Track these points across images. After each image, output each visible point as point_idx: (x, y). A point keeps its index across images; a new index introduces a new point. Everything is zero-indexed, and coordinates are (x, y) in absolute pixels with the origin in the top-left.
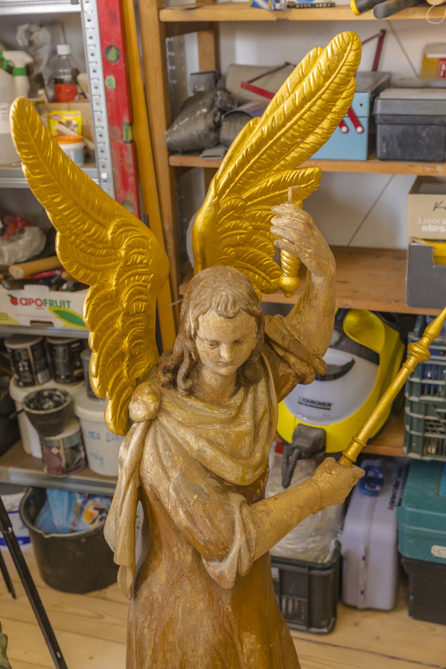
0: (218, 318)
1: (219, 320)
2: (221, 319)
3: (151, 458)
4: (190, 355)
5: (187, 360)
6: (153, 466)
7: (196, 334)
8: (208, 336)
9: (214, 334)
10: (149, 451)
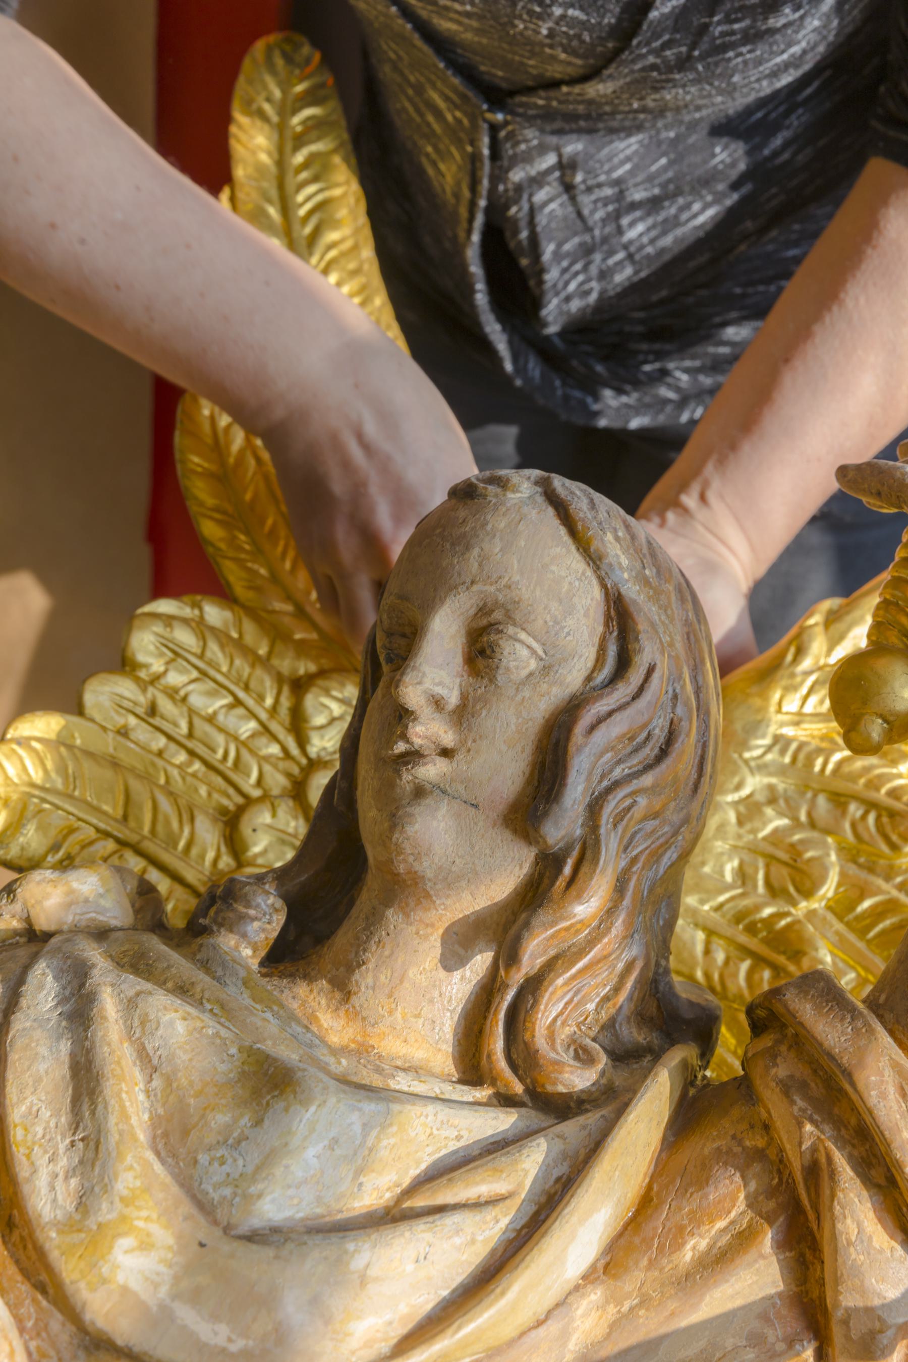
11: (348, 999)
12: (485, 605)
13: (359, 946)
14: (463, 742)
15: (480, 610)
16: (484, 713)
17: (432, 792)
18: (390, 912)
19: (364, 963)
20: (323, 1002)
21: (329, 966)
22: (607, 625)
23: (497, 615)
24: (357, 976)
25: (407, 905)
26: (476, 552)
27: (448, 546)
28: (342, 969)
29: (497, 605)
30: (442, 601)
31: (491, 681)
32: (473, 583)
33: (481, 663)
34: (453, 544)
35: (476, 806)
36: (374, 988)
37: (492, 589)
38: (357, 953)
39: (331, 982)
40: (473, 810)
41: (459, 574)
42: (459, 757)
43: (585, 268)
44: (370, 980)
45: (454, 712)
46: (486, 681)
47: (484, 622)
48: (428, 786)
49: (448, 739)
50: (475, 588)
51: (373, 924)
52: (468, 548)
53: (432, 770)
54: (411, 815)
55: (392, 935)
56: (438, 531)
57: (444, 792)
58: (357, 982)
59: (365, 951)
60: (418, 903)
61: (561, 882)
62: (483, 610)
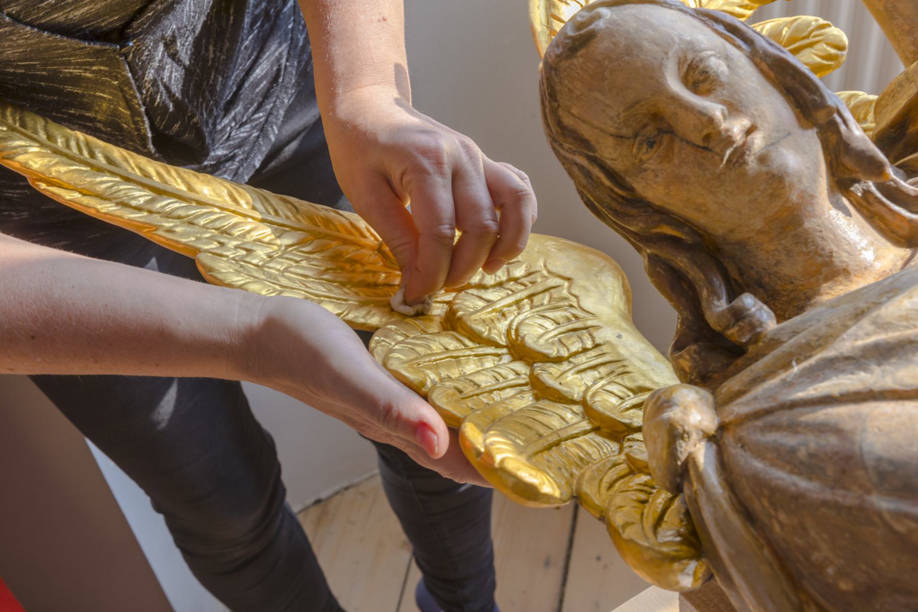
0: (575, 61)
1: (581, 60)
2: (582, 56)
3: (782, 516)
5: (682, 261)
6: (804, 529)
7: (611, 174)
8: (610, 123)
9: (608, 102)
10: (763, 506)
12: (679, 59)
13: (816, 253)
14: (753, 116)
15: (679, 63)
16: (743, 96)
17: (768, 151)
18: (807, 225)
19: (831, 253)
20: (841, 287)
21: (813, 280)
22: (708, 26)
23: (690, 56)
24: (836, 261)
25: (809, 212)
26: (646, 44)
27: (627, 58)
28: (824, 270)
30: (665, 78)
31: (720, 86)
32: (666, 53)
33: (704, 87)
34: (628, 55)
35: (789, 134)
36: (850, 254)
38: (821, 255)
39: (827, 279)
41: (655, 58)
42: (759, 123)
43: (204, 98)
44: (844, 255)
45: (730, 113)
46: (719, 89)
47: (686, 67)
48: (764, 151)
49: (746, 122)
50: (670, 54)
51: (806, 239)
52: (639, 47)
56: (606, 63)
57: (772, 144)
58: (841, 262)
59: (823, 249)
60: (812, 204)
61: (843, 128)
62: (680, 63)
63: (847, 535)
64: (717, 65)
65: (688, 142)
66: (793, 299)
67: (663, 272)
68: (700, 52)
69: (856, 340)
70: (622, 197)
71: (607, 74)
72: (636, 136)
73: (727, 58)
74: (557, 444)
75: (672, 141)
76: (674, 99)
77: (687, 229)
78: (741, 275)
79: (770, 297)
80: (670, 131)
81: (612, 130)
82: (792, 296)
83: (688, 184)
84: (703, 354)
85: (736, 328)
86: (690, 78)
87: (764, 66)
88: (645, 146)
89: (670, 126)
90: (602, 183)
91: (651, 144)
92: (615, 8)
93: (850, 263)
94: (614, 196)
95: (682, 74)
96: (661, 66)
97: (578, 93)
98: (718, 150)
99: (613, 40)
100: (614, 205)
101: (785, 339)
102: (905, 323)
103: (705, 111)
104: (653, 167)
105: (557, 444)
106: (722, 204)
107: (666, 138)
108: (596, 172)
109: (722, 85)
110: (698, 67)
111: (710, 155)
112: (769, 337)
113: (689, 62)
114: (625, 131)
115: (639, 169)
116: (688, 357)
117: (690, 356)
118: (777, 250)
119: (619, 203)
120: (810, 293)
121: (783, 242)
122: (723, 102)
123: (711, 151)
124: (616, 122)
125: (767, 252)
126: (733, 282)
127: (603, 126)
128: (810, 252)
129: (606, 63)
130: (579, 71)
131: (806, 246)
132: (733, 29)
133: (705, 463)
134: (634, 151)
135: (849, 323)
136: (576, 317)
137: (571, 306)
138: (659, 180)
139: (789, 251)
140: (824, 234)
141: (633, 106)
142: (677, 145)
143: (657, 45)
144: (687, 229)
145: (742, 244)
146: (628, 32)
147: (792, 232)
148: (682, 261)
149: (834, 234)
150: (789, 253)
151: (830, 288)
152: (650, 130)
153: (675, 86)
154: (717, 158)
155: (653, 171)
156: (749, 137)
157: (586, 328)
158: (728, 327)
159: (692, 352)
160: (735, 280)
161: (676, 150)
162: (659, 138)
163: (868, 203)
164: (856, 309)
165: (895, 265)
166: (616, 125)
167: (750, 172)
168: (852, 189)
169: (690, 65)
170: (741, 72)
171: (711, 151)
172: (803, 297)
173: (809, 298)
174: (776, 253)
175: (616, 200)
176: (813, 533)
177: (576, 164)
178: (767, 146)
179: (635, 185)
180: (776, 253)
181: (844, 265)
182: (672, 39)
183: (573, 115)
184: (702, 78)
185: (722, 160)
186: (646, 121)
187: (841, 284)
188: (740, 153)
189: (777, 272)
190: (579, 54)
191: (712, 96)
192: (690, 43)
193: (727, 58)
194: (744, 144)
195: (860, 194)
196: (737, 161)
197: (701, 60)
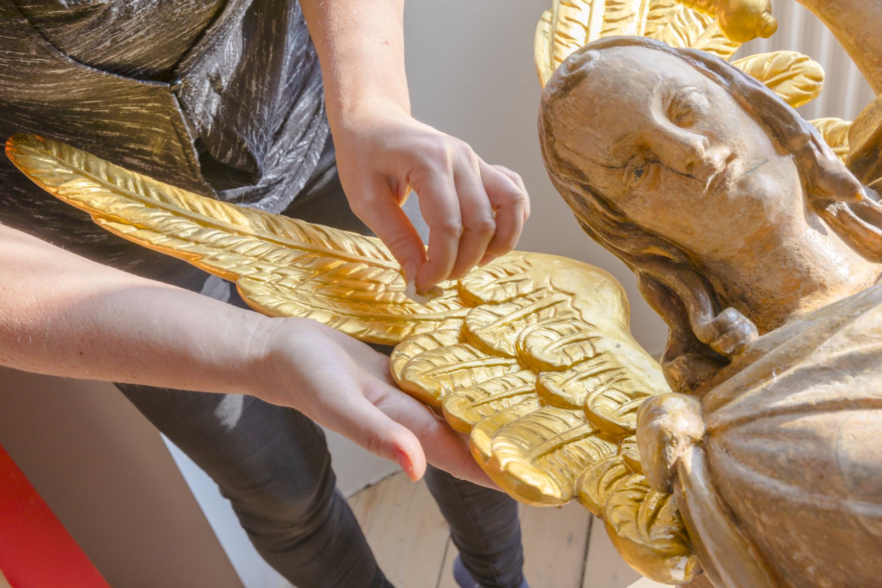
1: (573, 99)
2: (574, 94)
3: (764, 518)
4: (663, 261)
5: (670, 279)
6: (785, 530)
8: (600, 154)
9: (598, 136)
10: (747, 509)
11: (825, 286)
12: (663, 95)
13: (795, 269)
15: (663, 99)
16: (723, 127)
18: (785, 244)
19: (809, 269)
21: (792, 294)
22: (690, 63)
24: (814, 277)
26: (632, 82)
27: (615, 95)
28: (802, 285)
29: (668, 88)
31: (702, 118)
32: (651, 90)
33: (686, 119)
34: (616, 92)
35: (767, 161)
36: (826, 270)
37: (660, 84)
38: (799, 272)
39: (805, 294)
40: (768, 164)
41: (641, 95)
42: (738, 152)
45: (711, 142)
46: (700, 121)
47: (669, 102)
48: (743, 177)
49: (726, 151)
50: (655, 91)
51: (785, 257)
52: (626, 85)
53: (738, 169)
54: (760, 189)
55: (800, 248)
57: (751, 170)
58: (817, 277)
59: (801, 266)
60: (790, 225)
61: (817, 153)
62: (664, 99)
63: (825, 537)
64: (698, 99)
65: (673, 171)
66: (774, 312)
67: (653, 289)
68: (682, 88)
69: (832, 351)
70: (615, 222)
71: (597, 111)
72: (625, 166)
73: (708, 93)
74: (560, 447)
75: (658, 171)
76: (659, 132)
77: (674, 250)
78: (726, 290)
79: (753, 311)
80: (656, 161)
81: (603, 161)
82: (773, 309)
83: (674, 208)
84: (691, 364)
85: (721, 340)
86: (674, 112)
87: (742, 99)
88: (634, 175)
89: (657, 156)
90: (595, 209)
91: (639, 173)
92: (603, 51)
93: (826, 278)
94: (607, 221)
95: (666, 109)
96: (647, 102)
97: (572, 128)
98: (700, 177)
99: (603, 79)
100: (607, 228)
101: (766, 350)
102: (878, 336)
103: (687, 142)
104: (641, 194)
105: (560, 447)
106: (706, 226)
107: (653, 167)
108: (590, 199)
109: (703, 117)
110: (680, 102)
111: (693, 182)
112: (751, 348)
113: (672, 98)
114: (615, 162)
115: (629, 195)
116: (677, 367)
117: (680, 366)
118: (758, 267)
119: (612, 227)
120: (789, 306)
121: (763, 260)
122: (705, 133)
123: (694, 178)
124: (606, 154)
125: (749, 269)
126: (718, 297)
127: (595, 158)
128: (788, 269)
129: (596, 100)
130: (572, 108)
131: (785, 263)
132: (713, 66)
133: (693, 466)
134: (624, 179)
135: (826, 335)
136: (579, 329)
137: (574, 319)
138: (647, 205)
139: (769, 268)
140: (802, 252)
141: (621, 139)
142: (663, 173)
143: (642, 83)
144: (674, 250)
145: (725, 262)
146: (615, 72)
147: (772, 251)
148: (670, 279)
149: (811, 252)
150: (769, 270)
151: (808, 302)
152: (638, 161)
153: (660, 119)
154: (700, 184)
155: (642, 197)
156: (729, 165)
157: (588, 339)
158: (713, 340)
159: (681, 363)
160: (721, 296)
161: (662, 178)
162: (646, 167)
163: (843, 222)
164: (831, 322)
165: (869, 279)
166: (606, 157)
167: (731, 197)
168: (828, 209)
169: (673, 100)
170: (721, 105)
171: (694, 178)
172: (783, 310)
173: (788, 311)
174: (757, 269)
175: (609, 224)
176: (793, 534)
177: (572, 192)
178: (747, 172)
179: (625, 211)
180: (757, 269)
181: (821, 281)
182: (656, 77)
183: (568, 149)
184: (684, 111)
185: (705, 186)
186: (634, 152)
187: (818, 297)
188: (721, 180)
189: (759, 288)
190: (571, 93)
191: (695, 127)
192: (673, 80)
193: (708, 93)
194: (725, 171)
195: (835, 214)
196: (719, 187)
197: (684, 95)
